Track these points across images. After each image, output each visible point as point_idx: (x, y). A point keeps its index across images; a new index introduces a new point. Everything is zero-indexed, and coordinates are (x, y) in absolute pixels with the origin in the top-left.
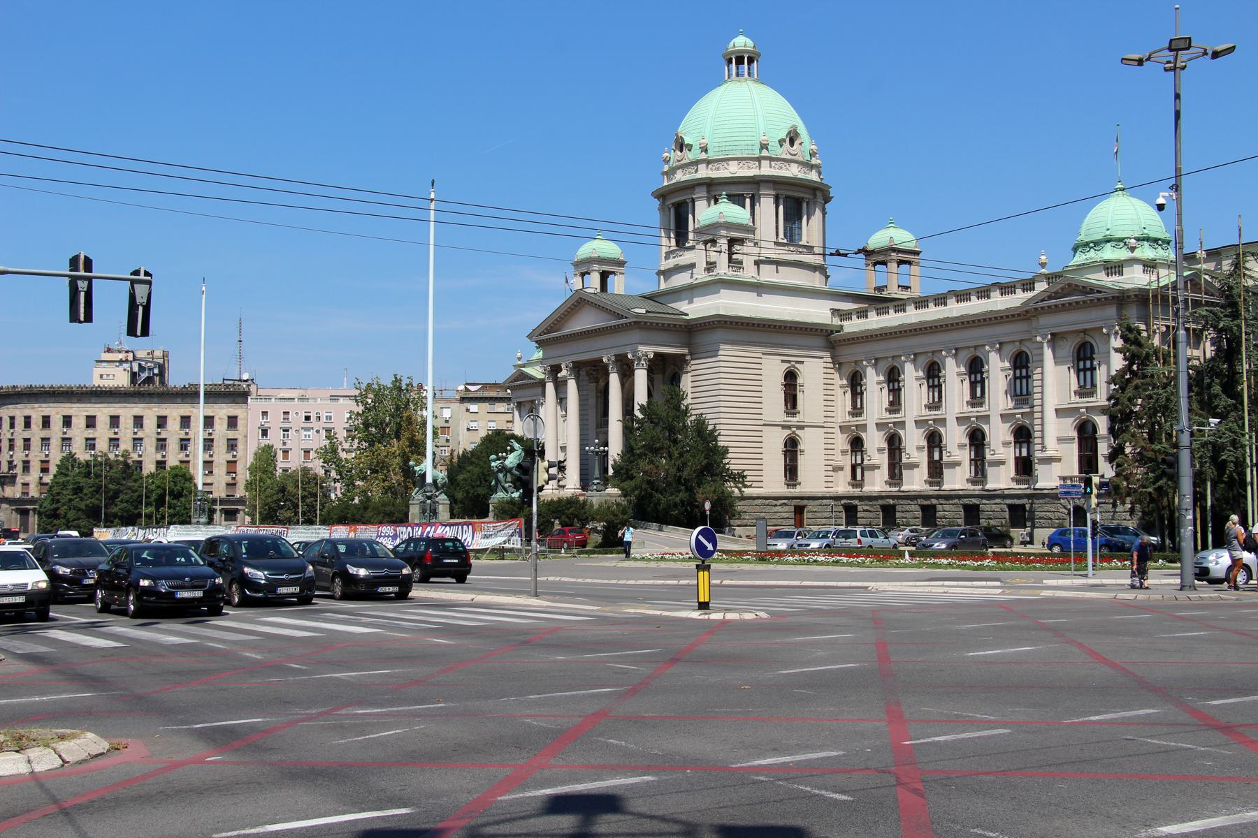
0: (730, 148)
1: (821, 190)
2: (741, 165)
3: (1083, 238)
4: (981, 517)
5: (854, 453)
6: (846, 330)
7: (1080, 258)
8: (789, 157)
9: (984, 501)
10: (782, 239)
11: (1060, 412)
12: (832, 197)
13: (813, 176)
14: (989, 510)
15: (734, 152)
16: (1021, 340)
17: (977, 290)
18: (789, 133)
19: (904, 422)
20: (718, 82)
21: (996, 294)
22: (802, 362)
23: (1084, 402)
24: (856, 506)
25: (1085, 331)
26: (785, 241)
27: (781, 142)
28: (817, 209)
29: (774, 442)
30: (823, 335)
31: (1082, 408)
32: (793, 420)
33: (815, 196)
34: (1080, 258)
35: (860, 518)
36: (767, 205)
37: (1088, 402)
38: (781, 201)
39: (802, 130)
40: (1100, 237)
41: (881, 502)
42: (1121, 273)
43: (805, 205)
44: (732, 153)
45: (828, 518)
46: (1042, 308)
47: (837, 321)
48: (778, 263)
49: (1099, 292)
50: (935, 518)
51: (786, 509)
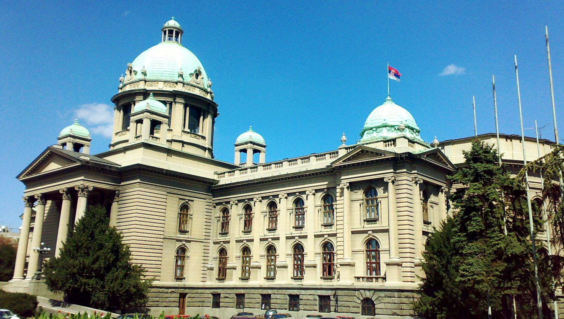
2: (166, 84)
3: (366, 126)
6: (221, 183)
8: (195, 84)
10: (187, 129)
12: (219, 114)
13: (208, 97)
15: (162, 77)
20: (156, 42)
22: (193, 201)
25: (371, 181)
27: (191, 75)
28: (209, 116)
32: (182, 237)
36: (179, 110)
38: (188, 108)
39: (203, 70)
40: (379, 124)
42: (394, 144)
48: (183, 143)
51: (174, 295)
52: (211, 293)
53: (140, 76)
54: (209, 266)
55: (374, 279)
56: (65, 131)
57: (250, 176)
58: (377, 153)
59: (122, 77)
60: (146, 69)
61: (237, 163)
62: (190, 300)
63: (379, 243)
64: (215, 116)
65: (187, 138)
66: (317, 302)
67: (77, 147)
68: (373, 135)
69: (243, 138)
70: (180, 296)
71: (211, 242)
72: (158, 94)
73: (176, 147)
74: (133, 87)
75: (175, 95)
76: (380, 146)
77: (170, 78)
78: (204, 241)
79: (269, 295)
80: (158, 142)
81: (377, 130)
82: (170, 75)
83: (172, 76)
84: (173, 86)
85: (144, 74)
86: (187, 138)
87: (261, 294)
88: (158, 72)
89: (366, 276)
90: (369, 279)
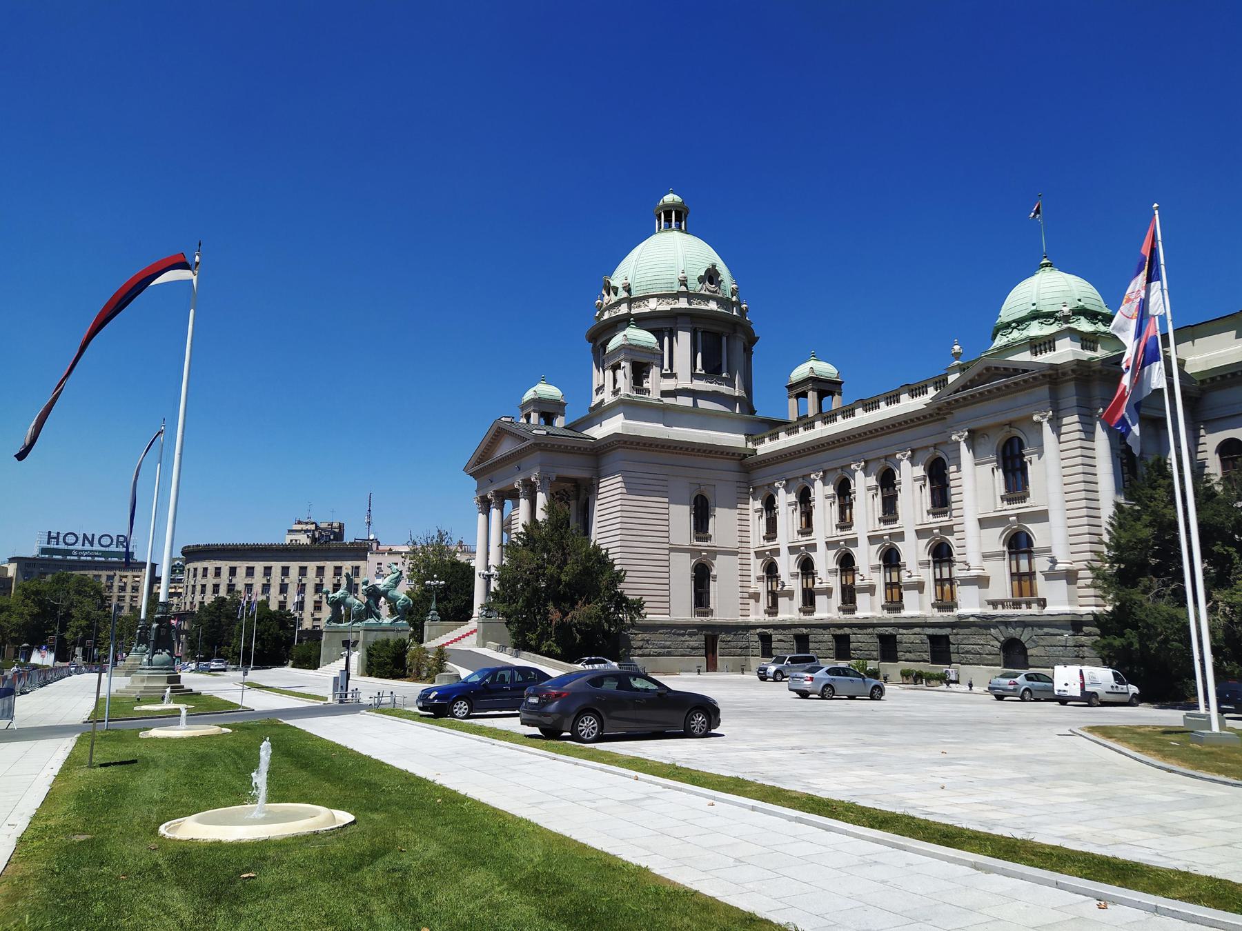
0: (651, 287)
1: (741, 325)
2: (661, 301)
4: (898, 650)
5: (770, 580)
6: (759, 453)
7: (1000, 341)
9: (901, 631)
11: (984, 523)
14: (907, 641)
15: (654, 290)
16: (936, 444)
17: (885, 396)
18: (708, 271)
19: (816, 544)
21: (905, 398)
23: (1014, 509)
24: (771, 635)
25: (1010, 424)
26: (703, 372)
27: (701, 280)
29: (683, 567)
30: (734, 459)
31: (1012, 516)
33: (735, 331)
34: (1000, 341)
35: (775, 648)
36: (684, 339)
37: (1020, 508)
39: (722, 268)
40: (1025, 313)
41: (794, 631)
43: (724, 339)
44: (652, 290)
45: (744, 648)
46: (956, 401)
47: (750, 445)
48: (695, 394)
49: (1025, 371)
50: (849, 649)
52: (757, 634)
53: (623, 294)
54: (751, 590)
55: (1024, 606)
56: (529, 395)
57: (803, 436)
58: (1016, 370)
59: (599, 301)
60: (629, 281)
61: (793, 416)
62: (723, 644)
63: (1032, 537)
64: (752, 340)
65: (700, 385)
66: (927, 647)
67: (548, 418)
68: (1011, 336)
69: (800, 372)
70: (706, 638)
71: (752, 551)
72: (642, 321)
73: (686, 402)
74: (613, 313)
75: (675, 315)
76: (1025, 357)
77: (666, 289)
78: (739, 550)
79: (847, 636)
80: (647, 396)
81: (1019, 326)
82: (666, 285)
83: (669, 285)
84: (673, 302)
85: (628, 289)
86: (700, 385)
87: (833, 635)
88: (649, 283)
89: (1009, 597)
90: (1017, 605)
